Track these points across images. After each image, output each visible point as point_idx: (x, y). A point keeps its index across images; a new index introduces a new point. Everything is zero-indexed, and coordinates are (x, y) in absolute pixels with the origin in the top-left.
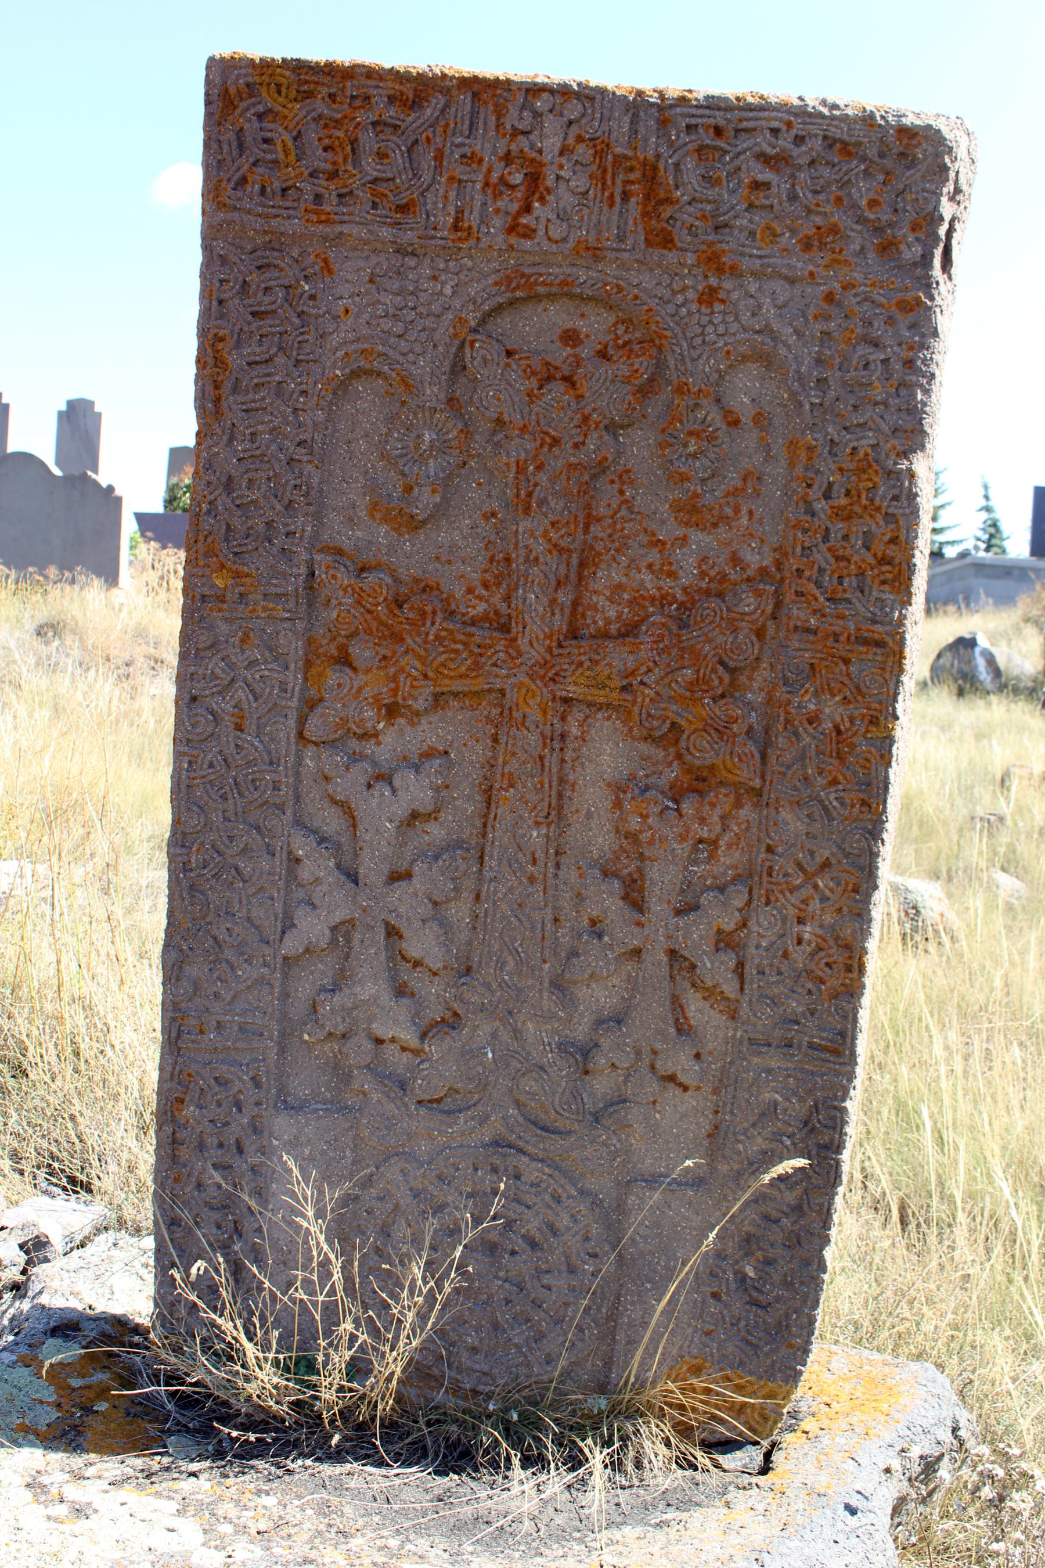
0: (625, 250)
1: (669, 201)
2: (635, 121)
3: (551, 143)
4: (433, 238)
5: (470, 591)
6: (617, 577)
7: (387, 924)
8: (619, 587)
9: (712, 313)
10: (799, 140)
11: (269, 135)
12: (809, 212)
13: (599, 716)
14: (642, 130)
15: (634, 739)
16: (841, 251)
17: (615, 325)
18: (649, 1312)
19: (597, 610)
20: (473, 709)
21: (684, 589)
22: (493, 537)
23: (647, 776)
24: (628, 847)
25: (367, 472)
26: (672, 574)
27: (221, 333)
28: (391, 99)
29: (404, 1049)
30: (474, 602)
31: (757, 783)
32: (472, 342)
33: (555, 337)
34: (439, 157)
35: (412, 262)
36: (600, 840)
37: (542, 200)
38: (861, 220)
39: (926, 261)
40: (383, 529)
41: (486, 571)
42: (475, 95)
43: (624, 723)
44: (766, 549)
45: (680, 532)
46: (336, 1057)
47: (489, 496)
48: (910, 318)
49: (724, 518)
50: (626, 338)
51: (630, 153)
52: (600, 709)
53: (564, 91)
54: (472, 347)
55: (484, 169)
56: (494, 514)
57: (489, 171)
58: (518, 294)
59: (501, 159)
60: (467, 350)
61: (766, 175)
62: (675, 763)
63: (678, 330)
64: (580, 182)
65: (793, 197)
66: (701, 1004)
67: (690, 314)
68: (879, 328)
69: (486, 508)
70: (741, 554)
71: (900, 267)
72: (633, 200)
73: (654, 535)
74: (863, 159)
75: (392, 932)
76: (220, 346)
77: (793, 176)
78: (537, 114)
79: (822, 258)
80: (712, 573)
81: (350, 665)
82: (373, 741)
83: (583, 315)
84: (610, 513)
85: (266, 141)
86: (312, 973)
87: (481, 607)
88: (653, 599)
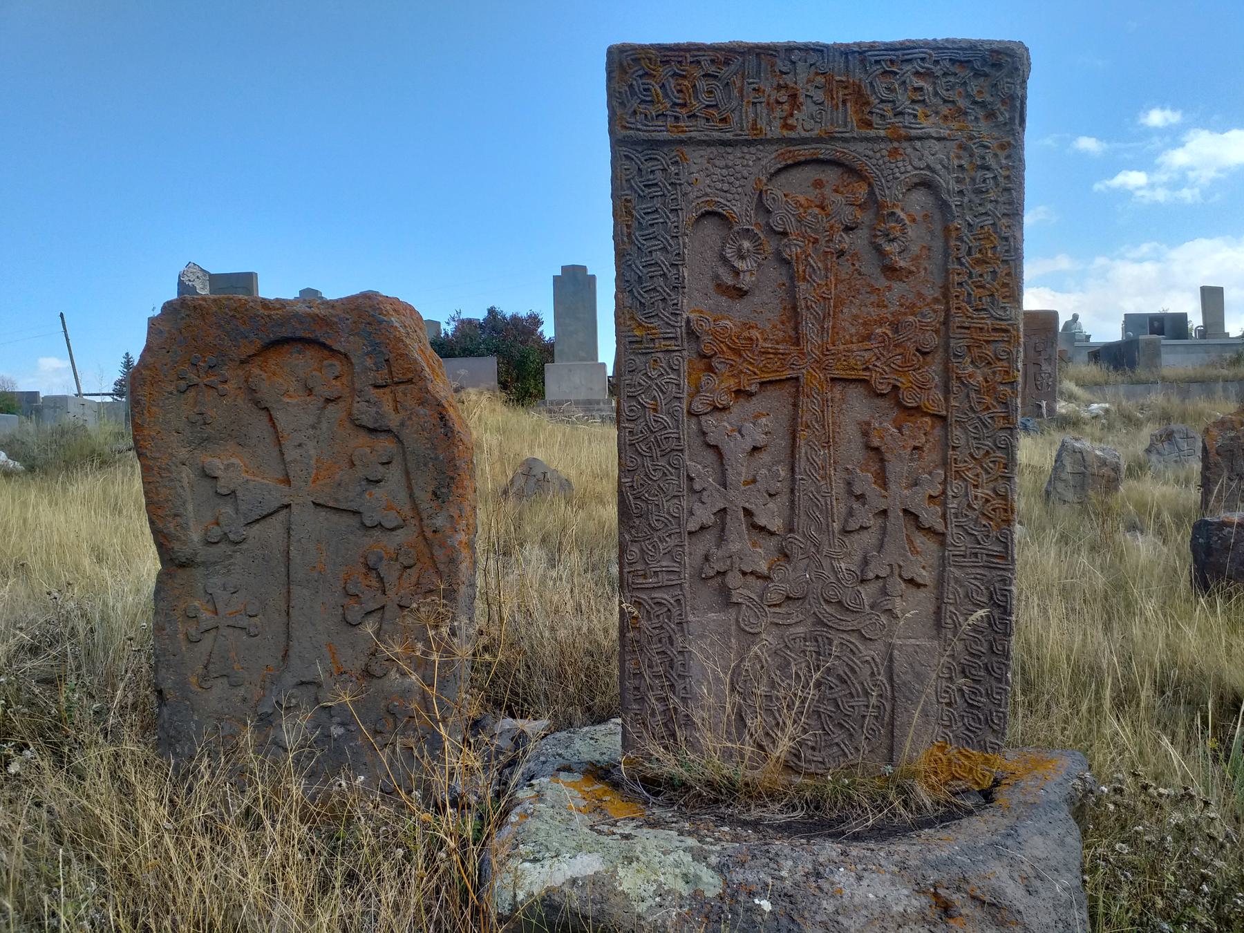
1: (868, 103)
3: (802, 77)
5: (775, 327)
7: (744, 509)
8: (855, 317)
10: (937, 62)
18: (911, 716)
26: (886, 306)
28: (712, 61)
29: (758, 577)
31: (944, 413)
34: (741, 90)
38: (975, 103)
39: (1012, 119)
42: (758, 55)
45: (887, 283)
48: (1006, 152)
49: (911, 272)
51: (844, 79)
53: (807, 49)
58: (789, 162)
61: (921, 83)
64: (819, 96)
65: (936, 94)
68: (991, 161)
72: (849, 104)
74: (973, 69)
75: (748, 513)
77: (934, 83)
78: (794, 63)
79: (955, 125)
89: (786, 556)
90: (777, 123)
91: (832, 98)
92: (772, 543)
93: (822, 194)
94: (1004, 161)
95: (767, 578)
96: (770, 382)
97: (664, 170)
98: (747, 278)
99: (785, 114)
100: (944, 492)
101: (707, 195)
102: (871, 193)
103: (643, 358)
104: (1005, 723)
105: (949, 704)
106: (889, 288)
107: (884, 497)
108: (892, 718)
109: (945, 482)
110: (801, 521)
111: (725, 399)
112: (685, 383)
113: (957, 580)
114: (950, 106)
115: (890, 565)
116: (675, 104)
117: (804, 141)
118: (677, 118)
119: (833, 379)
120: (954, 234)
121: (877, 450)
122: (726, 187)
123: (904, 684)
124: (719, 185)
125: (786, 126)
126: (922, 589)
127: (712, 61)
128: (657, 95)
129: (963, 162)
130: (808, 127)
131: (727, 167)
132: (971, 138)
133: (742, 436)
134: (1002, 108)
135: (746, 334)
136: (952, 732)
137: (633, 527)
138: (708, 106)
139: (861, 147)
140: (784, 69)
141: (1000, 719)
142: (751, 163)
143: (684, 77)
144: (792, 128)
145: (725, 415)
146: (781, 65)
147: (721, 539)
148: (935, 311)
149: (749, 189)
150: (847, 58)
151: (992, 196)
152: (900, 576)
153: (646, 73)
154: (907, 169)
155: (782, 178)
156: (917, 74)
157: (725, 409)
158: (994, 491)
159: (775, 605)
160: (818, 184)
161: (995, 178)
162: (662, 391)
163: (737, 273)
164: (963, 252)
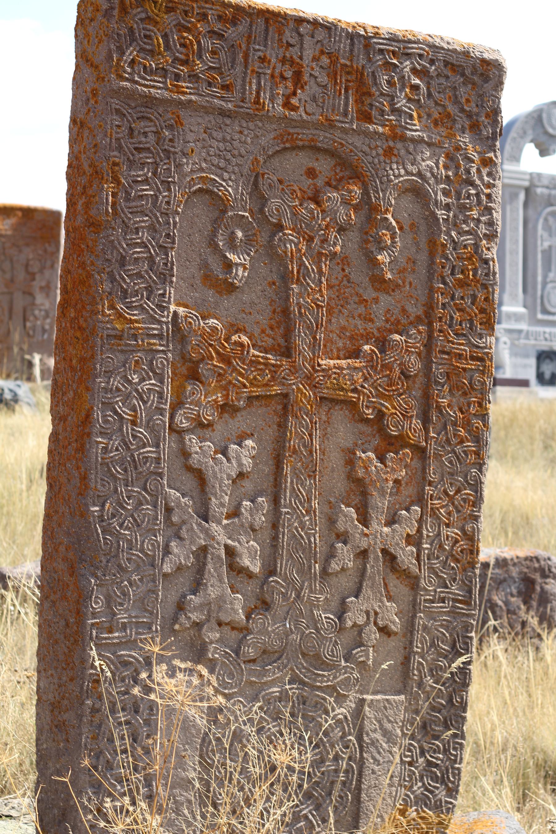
0: (346, 122)
1: (370, 94)
2: (352, 44)
3: (308, 54)
4: (243, 107)
5: (263, 331)
6: (343, 322)
8: (343, 329)
9: (392, 162)
11: (148, 33)
12: (436, 104)
13: (337, 408)
14: (356, 50)
15: (355, 421)
16: (451, 128)
17: (335, 166)
19: (332, 342)
20: (266, 406)
21: (378, 329)
22: (274, 297)
23: (363, 444)
24: (354, 488)
25: (201, 255)
26: (371, 320)
27: (117, 160)
28: (220, 17)
29: (233, 628)
30: (266, 338)
32: (263, 175)
33: (303, 172)
35: (228, 121)
36: (339, 485)
37: (302, 88)
38: (462, 110)
40: (211, 292)
41: (271, 319)
42: (267, 21)
43: (350, 411)
44: (419, 305)
45: (374, 295)
46: (192, 639)
47: (271, 271)
49: (398, 286)
50: (341, 174)
51: (348, 63)
52: (337, 404)
53: (315, 23)
54: (263, 178)
55: (271, 67)
56: (274, 283)
57: (274, 68)
58: (288, 145)
59: (280, 61)
60: (260, 179)
62: (377, 436)
63: (373, 172)
64: (323, 79)
66: (397, 582)
67: (380, 162)
69: (270, 279)
70: (406, 307)
71: (481, 139)
72: (350, 92)
73: (361, 296)
76: (117, 168)
78: (300, 35)
79: (443, 131)
80: (392, 319)
81: (198, 379)
82: (210, 429)
83: (317, 159)
84: (338, 282)
85: (146, 36)
86: (176, 584)
87: (270, 341)
88: (362, 335)
89: (264, 602)
90: (280, 100)
91: (336, 83)
92: (251, 587)
93: (315, 184)
94: (486, 178)
95: (245, 630)
96: (257, 397)
97: (156, 133)
98: (240, 273)
99: (289, 91)
100: (419, 531)
101: (202, 170)
102: (366, 193)
103: (122, 357)
104: (459, 779)
105: (410, 764)
106: (376, 300)
107: (366, 535)
108: (359, 781)
109: (420, 521)
110: (283, 565)
111: (209, 415)
112: (168, 389)
113: (425, 628)
114: (440, 109)
115: (367, 613)
116: (176, 59)
117: (303, 124)
118: (177, 77)
119: (321, 398)
120: (440, 249)
121: (359, 481)
122: (222, 164)
123: (373, 743)
124: (216, 161)
125: (287, 105)
126: (392, 637)
127: (220, 17)
128: (159, 44)
129: (450, 173)
130: (309, 110)
131: (224, 140)
132: (458, 148)
133: (228, 460)
134: (486, 121)
135: (235, 338)
136: (413, 792)
137: (97, 568)
138: (211, 68)
139: (358, 141)
140: (292, 41)
141: (454, 775)
142: (249, 140)
143: (188, 30)
144: (294, 109)
145: (208, 433)
146: (289, 36)
147: (197, 586)
148: (419, 332)
149: (245, 171)
150: (352, 40)
151: (475, 213)
152: (375, 623)
153: (148, 18)
154: (399, 174)
155: (276, 162)
156: (414, 71)
157: (210, 425)
158: (463, 530)
159: (253, 661)
160: (311, 173)
161: (477, 195)
162: (142, 399)
163: (229, 265)
164: (447, 271)
